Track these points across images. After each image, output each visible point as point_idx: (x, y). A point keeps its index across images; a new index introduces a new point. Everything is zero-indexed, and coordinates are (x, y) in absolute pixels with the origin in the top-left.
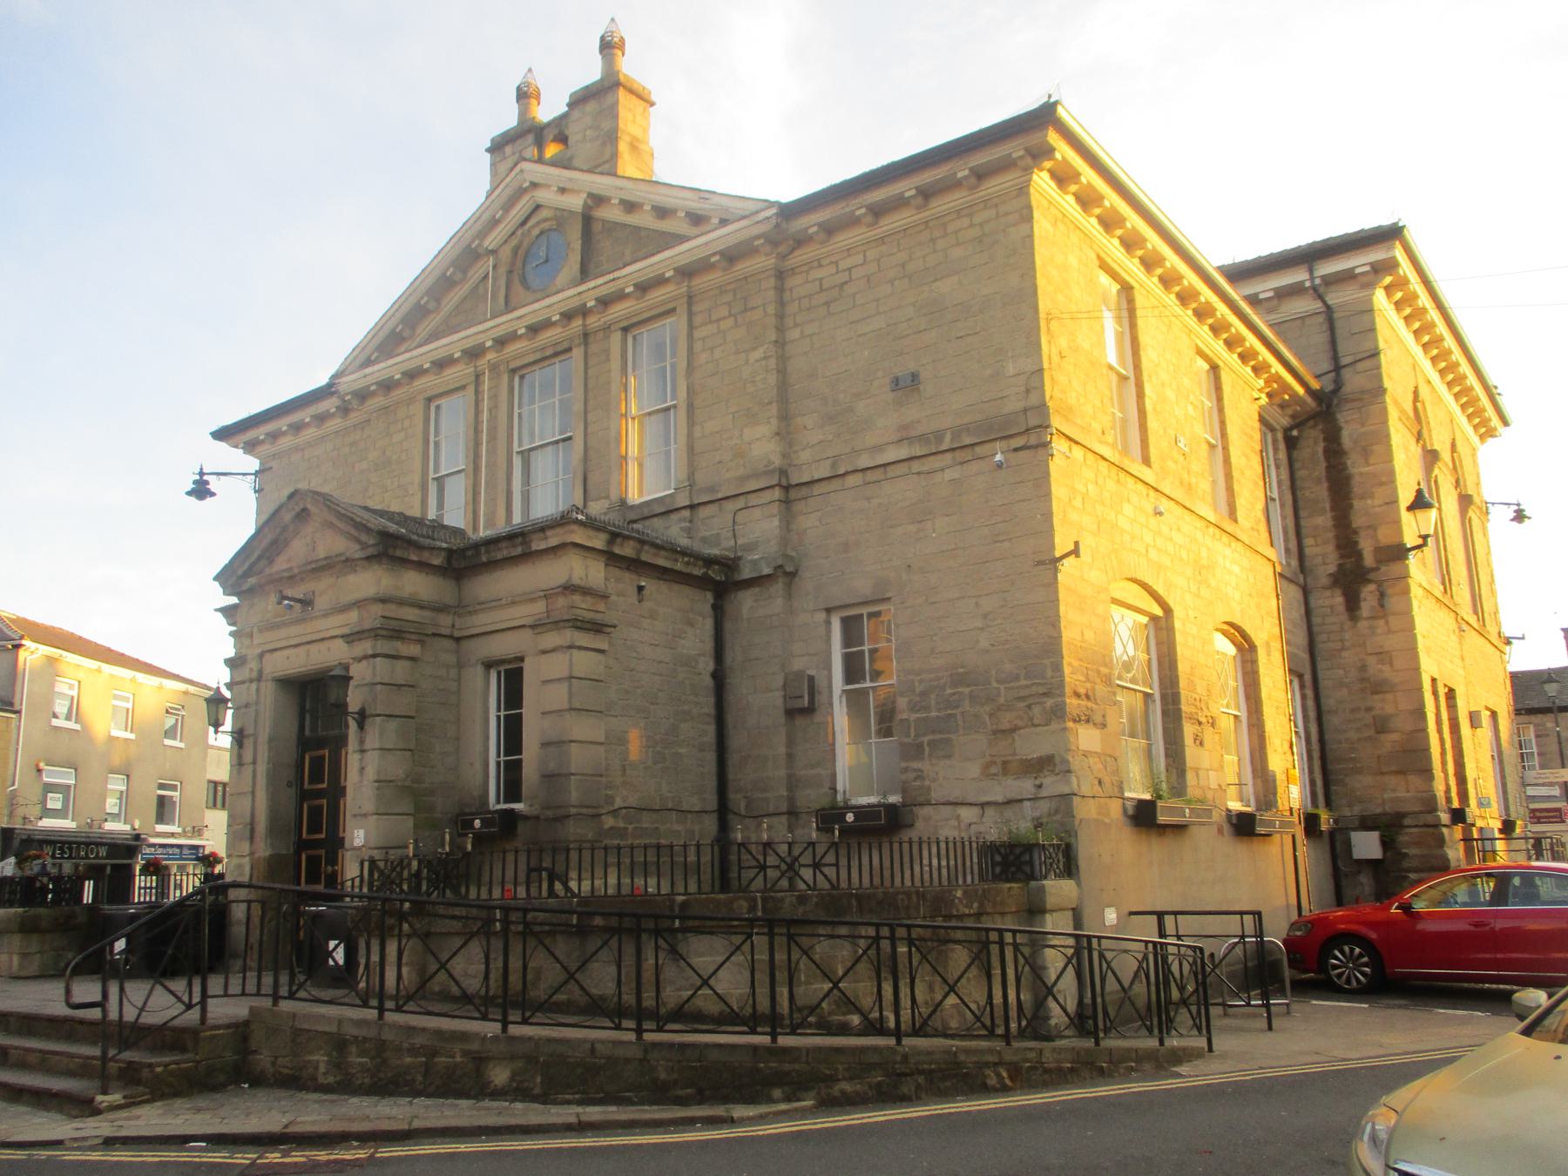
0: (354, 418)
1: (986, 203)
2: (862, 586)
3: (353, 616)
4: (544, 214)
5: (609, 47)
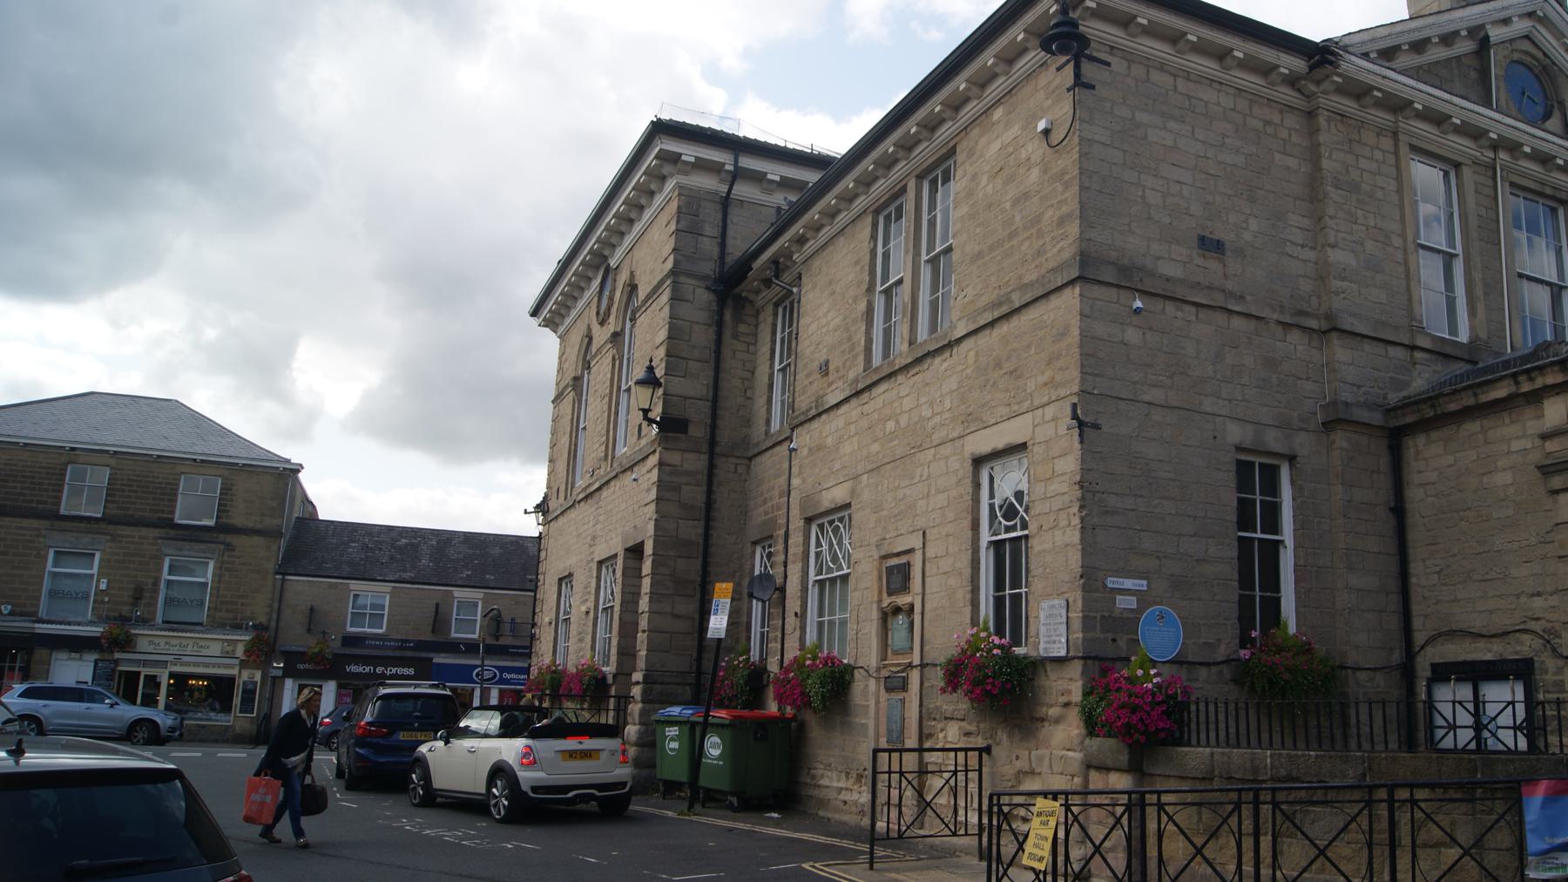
0: (1286, 94)
4: (1526, 46)
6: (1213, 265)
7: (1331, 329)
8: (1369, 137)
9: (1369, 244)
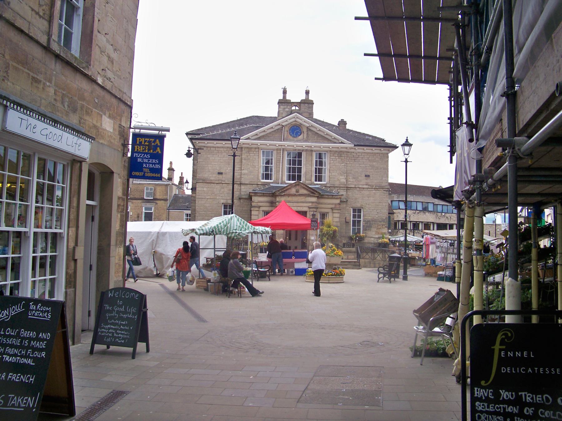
1: (382, 153)
2: (358, 205)
3: (310, 204)
5: (307, 93)
6: (220, 176)
7: (241, 184)
8: (253, 150)
9: (251, 168)
